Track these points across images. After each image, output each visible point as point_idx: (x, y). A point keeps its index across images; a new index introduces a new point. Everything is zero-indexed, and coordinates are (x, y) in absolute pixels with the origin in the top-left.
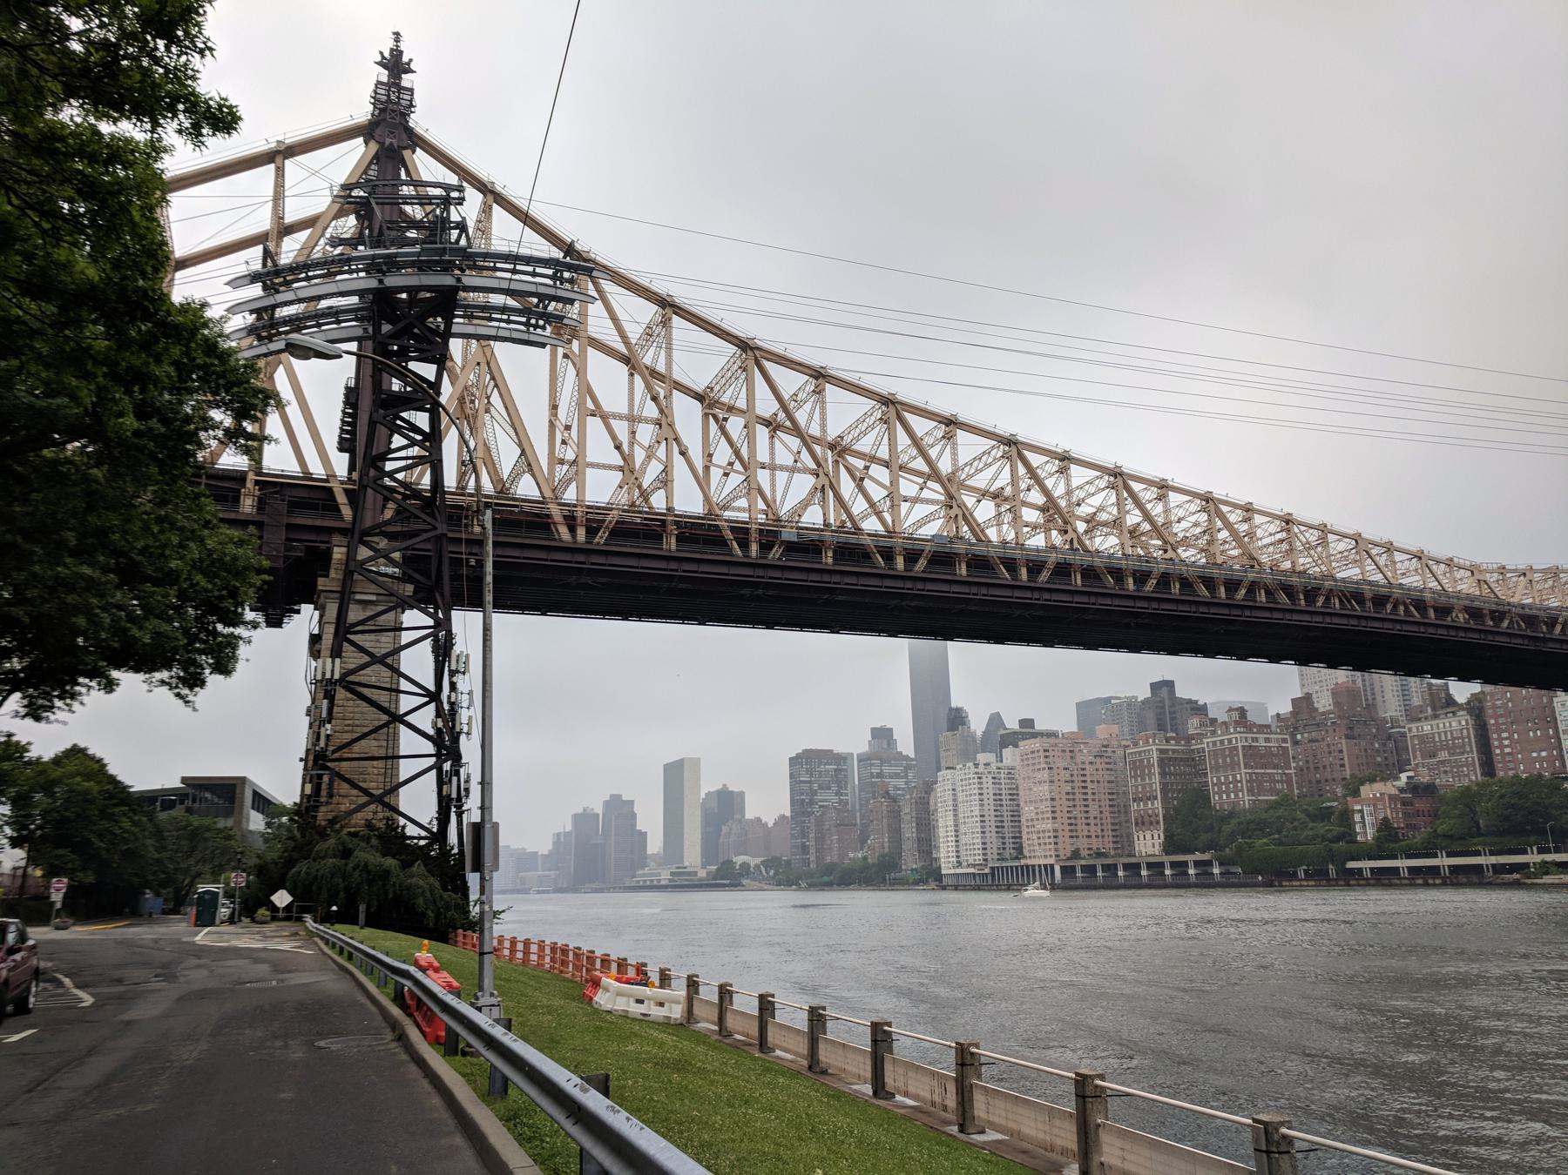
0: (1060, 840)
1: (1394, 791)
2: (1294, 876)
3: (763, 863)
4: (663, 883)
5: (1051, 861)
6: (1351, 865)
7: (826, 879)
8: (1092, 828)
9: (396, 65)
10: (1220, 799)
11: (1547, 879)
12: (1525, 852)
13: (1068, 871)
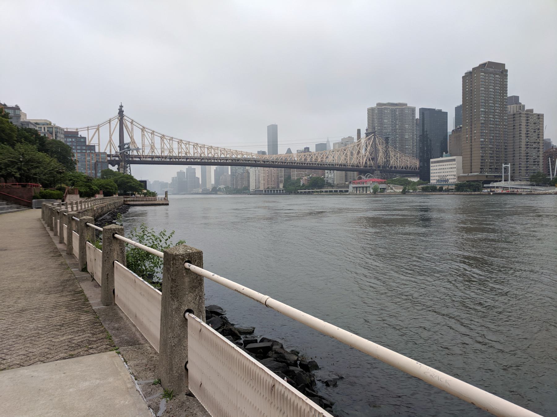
0: (265, 185)
1: (307, 178)
2: (292, 193)
3: (225, 188)
4: (200, 192)
5: (263, 189)
6: (298, 191)
7: (234, 192)
8: (272, 182)
9: (121, 106)
10: (292, 178)
11: (314, 194)
12: (314, 189)
13: (265, 191)
